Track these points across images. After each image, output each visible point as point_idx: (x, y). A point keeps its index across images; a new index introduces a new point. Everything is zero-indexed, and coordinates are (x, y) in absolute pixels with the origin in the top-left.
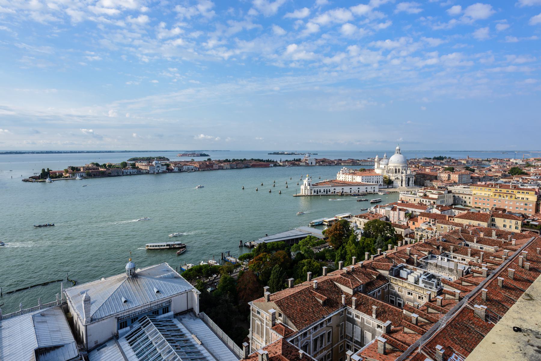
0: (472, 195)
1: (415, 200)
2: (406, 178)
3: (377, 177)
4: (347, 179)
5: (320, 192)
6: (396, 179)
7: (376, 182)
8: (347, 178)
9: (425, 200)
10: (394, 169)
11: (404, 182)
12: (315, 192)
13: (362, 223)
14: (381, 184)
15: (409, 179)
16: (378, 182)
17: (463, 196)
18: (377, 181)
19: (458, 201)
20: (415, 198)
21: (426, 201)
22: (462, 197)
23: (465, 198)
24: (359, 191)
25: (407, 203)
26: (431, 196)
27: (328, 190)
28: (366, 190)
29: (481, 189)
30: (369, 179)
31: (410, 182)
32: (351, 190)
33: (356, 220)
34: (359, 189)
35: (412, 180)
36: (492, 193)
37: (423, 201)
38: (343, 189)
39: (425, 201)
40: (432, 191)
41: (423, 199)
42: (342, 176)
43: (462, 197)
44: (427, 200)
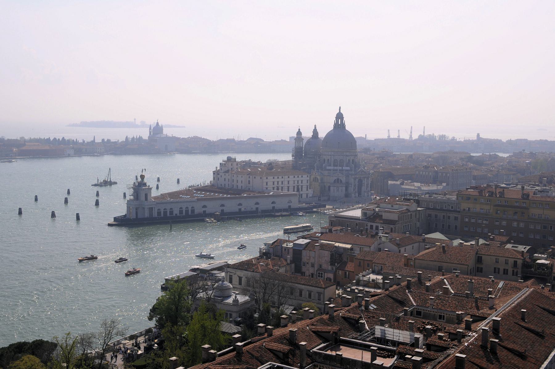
0: (459, 212)
2: (355, 179)
3: (296, 179)
5: (171, 213)
7: (296, 189)
11: (351, 189)
12: (159, 213)
13: (244, 280)
15: (360, 181)
16: (300, 190)
18: (298, 186)
22: (444, 216)
23: (449, 217)
27: (190, 209)
30: (280, 183)
31: (364, 188)
33: (231, 274)
35: (367, 184)
37: (372, 227)
39: (374, 228)
41: (372, 224)
44: (379, 225)
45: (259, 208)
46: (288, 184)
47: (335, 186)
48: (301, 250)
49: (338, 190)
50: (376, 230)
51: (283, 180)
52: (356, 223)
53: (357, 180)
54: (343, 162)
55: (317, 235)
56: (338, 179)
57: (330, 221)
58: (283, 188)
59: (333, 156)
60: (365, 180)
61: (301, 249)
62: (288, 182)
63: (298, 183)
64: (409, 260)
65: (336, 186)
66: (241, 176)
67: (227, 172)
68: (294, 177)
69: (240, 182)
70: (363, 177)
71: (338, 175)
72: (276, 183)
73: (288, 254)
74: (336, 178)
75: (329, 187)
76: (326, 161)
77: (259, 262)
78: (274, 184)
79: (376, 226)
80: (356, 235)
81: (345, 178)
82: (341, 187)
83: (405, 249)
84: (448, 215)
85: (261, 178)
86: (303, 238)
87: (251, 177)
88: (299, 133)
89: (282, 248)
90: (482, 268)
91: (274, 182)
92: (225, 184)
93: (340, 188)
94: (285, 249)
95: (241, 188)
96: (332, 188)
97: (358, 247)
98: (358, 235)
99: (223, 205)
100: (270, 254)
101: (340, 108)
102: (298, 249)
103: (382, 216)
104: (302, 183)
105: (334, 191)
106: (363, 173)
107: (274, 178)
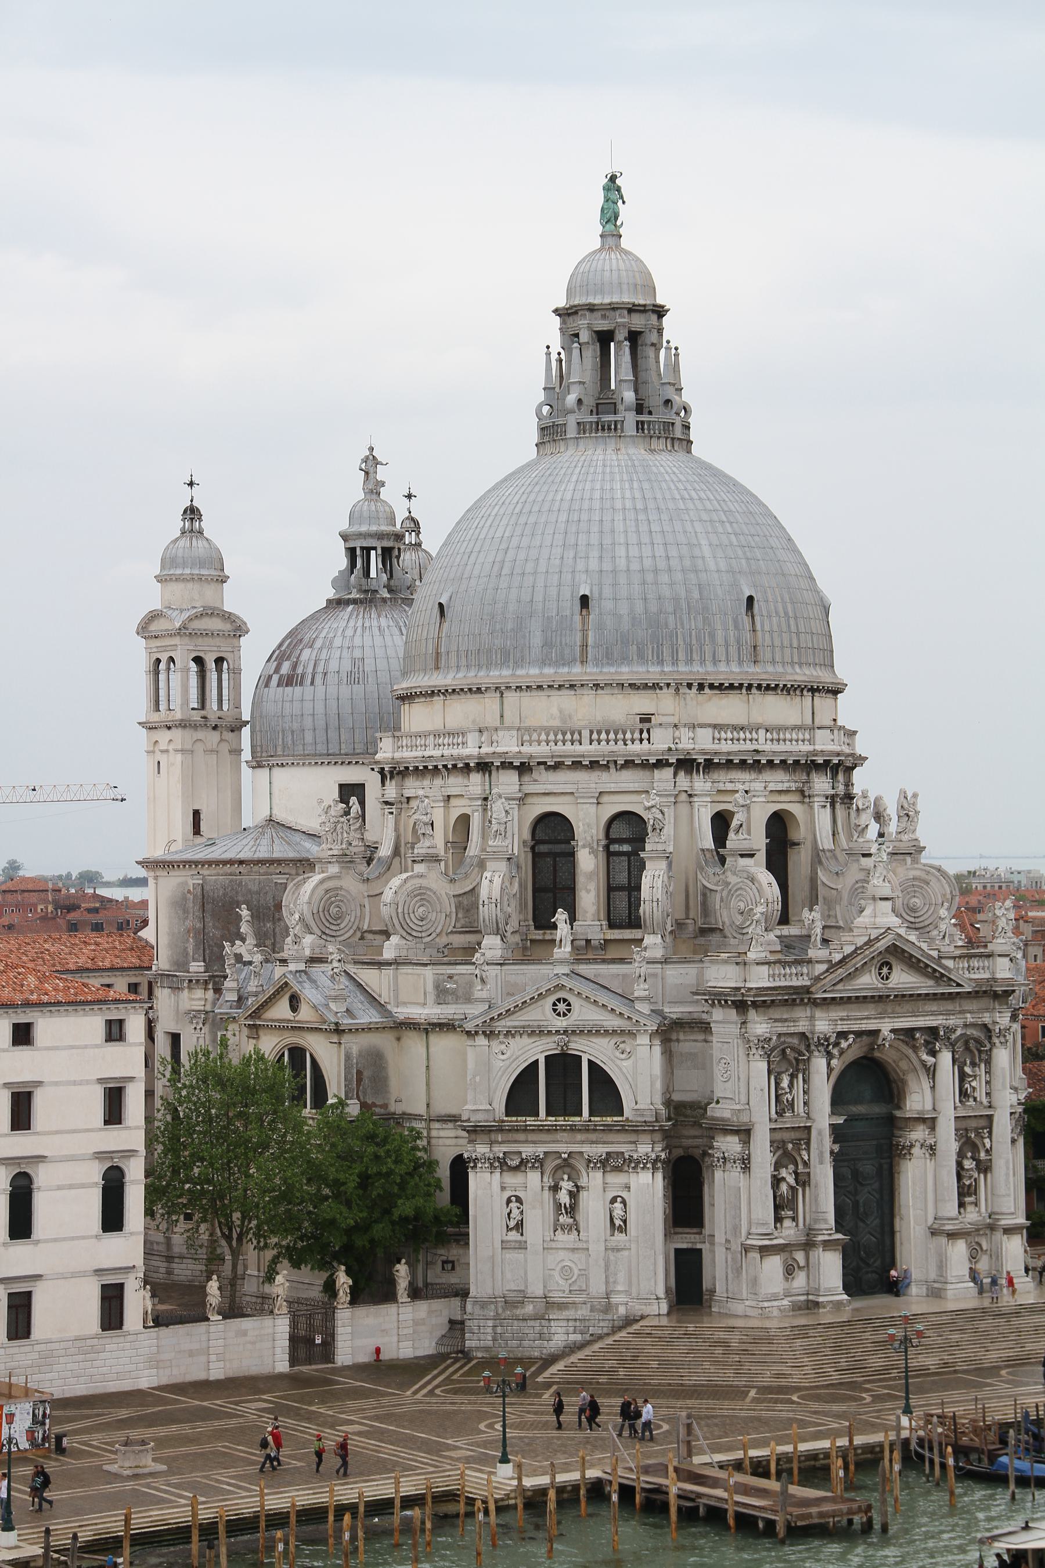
60: (931, 1072)
74: (537, 1050)
82: (607, 1163)
105: (519, 1226)
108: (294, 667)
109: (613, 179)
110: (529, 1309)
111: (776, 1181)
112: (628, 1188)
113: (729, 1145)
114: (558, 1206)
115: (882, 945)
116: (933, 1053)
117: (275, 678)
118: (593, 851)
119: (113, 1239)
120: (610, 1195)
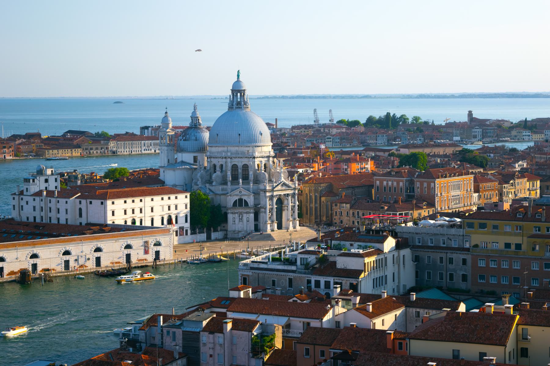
0: (468, 250)
1: (290, 280)
3: (166, 202)
4: (53, 215)
6: (235, 204)
8: (54, 209)
9: (322, 280)
10: (230, 165)
14: (181, 228)
15: (280, 201)
17: (444, 255)
19: (429, 274)
20: (291, 275)
21: (327, 284)
22: (441, 259)
23: (451, 261)
24: (98, 260)
25: (263, 295)
26: (342, 263)
28: (128, 256)
29: (495, 227)
30: (137, 211)
32: (67, 257)
34: (98, 254)
36: (525, 238)
37: (318, 283)
38: (34, 256)
40: (348, 243)
41: (318, 278)
42: (32, 203)
43: (441, 259)
44: (331, 280)
45: (102, 259)
46: (152, 211)
47: (236, 211)
48: (198, 332)
49: (241, 220)
50: (325, 288)
51: (141, 205)
52: (289, 278)
53: (275, 200)
54: (248, 170)
55: (223, 302)
56: (241, 200)
57: (241, 276)
58: (143, 219)
59: (229, 160)
60: (287, 200)
61: (198, 330)
62: (152, 209)
63: (169, 209)
64: (395, 340)
65: (237, 213)
66: (64, 200)
67: (39, 194)
68: (162, 199)
69: (62, 211)
70: (285, 195)
71: (240, 192)
72: (129, 212)
73: (174, 339)
74: (237, 198)
75: (226, 214)
76: (218, 168)
77: (123, 359)
78: (125, 213)
79: (325, 281)
80: (291, 300)
81: (252, 197)
82: (247, 213)
83: (383, 320)
84: (449, 255)
85: (102, 203)
86: (197, 310)
87: (84, 201)
88: (165, 120)
89: (162, 331)
90: (527, 349)
91: (125, 211)
92: (35, 218)
93: (245, 215)
94: (168, 332)
95: (150, 225)
96: (230, 216)
97: (300, 322)
98: (295, 299)
99: (34, 256)
100: (141, 342)
101: (238, 71)
102: (193, 330)
103: (335, 263)
104: (176, 209)
105: (234, 221)
106: (284, 188)
107: (125, 202)
108: (186, 138)
109: (239, 71)
110: (236, 232)
111: (269, 215)
112: (249, 216)
113: (263, 210)
114: (240, 219)
115: (282, 183)
116: (288, 197)
117: (182, 140)
118: (241, 170)
119: (187, 224)
120: (247, 216)
